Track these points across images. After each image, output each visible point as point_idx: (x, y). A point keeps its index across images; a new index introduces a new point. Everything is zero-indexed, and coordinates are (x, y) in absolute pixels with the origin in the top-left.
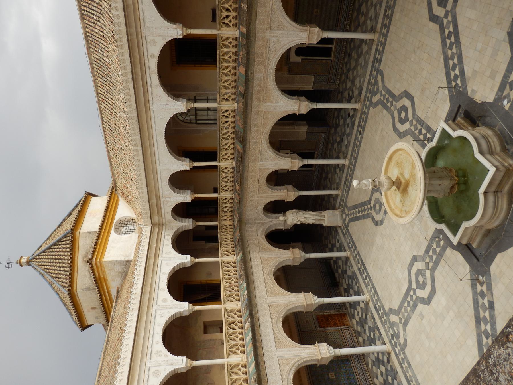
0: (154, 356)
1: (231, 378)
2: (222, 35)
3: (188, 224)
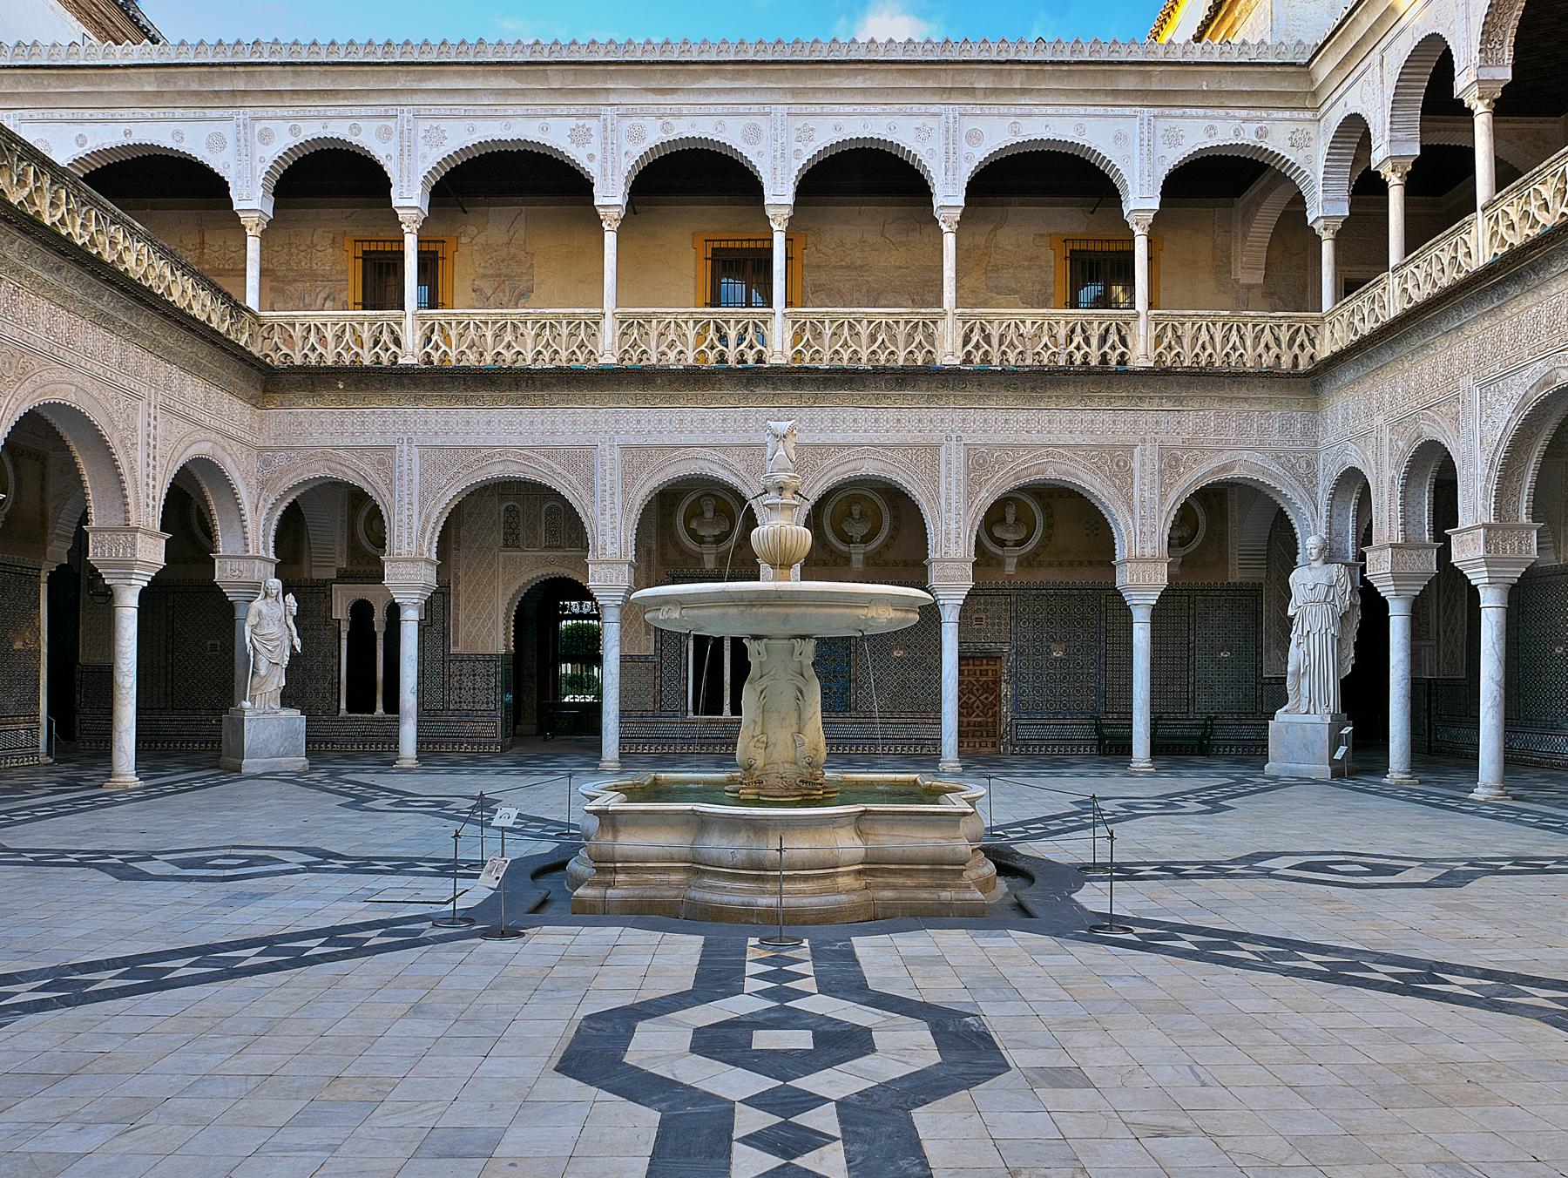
0: (799, 122)
1: (732, 323)
3: (1326, 205)
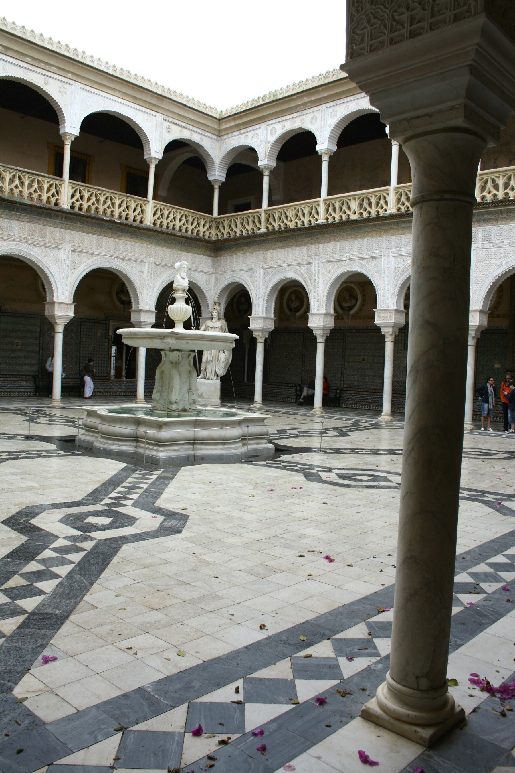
2: (63, 185)
